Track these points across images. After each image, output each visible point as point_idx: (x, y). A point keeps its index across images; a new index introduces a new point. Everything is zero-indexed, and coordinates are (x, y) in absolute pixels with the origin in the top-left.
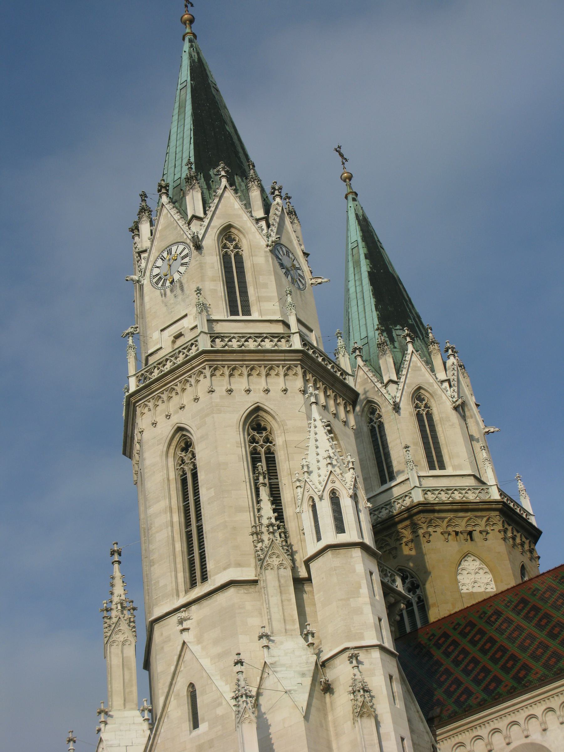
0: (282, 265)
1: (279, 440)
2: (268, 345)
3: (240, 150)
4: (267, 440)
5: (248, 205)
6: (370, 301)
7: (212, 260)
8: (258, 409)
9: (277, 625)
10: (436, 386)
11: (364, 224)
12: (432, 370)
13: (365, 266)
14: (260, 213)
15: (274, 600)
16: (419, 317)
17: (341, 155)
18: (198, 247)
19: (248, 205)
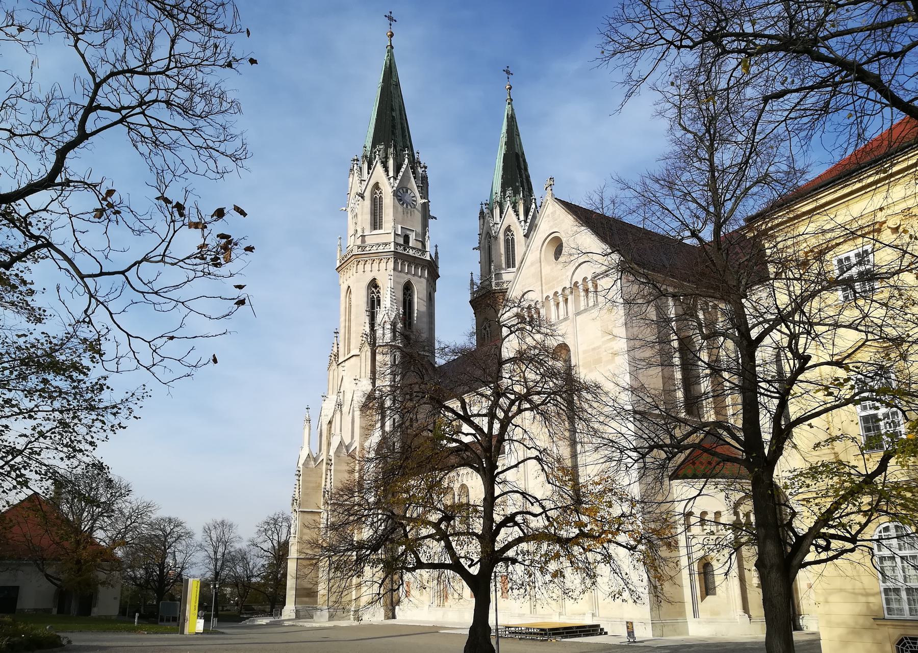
0: (400, 200)
1: (381, 291)
2: (381, 249)
3: (399, 126)
4: (378, 292)
5: (387, 171)
6: (501, 173)
7: (367, 203)
8: (375, 279)
9: (363, 375)
10: (518, 224)
11: (512, 120)
12: (517, 215)
13: (503, 152)
14: (391, 174)
15: (363, 365)
16: (528, 177)
17: (508, 72)
18: (363, 197)
19: (387, 171)
